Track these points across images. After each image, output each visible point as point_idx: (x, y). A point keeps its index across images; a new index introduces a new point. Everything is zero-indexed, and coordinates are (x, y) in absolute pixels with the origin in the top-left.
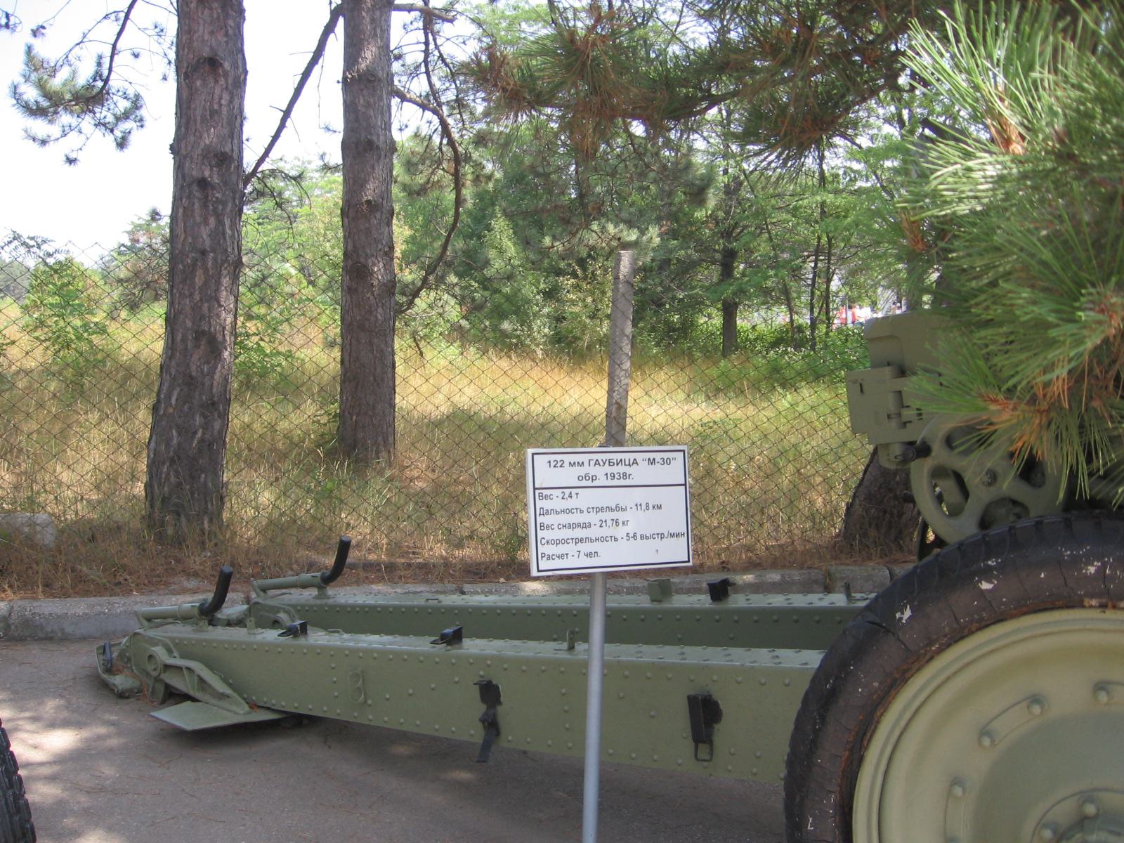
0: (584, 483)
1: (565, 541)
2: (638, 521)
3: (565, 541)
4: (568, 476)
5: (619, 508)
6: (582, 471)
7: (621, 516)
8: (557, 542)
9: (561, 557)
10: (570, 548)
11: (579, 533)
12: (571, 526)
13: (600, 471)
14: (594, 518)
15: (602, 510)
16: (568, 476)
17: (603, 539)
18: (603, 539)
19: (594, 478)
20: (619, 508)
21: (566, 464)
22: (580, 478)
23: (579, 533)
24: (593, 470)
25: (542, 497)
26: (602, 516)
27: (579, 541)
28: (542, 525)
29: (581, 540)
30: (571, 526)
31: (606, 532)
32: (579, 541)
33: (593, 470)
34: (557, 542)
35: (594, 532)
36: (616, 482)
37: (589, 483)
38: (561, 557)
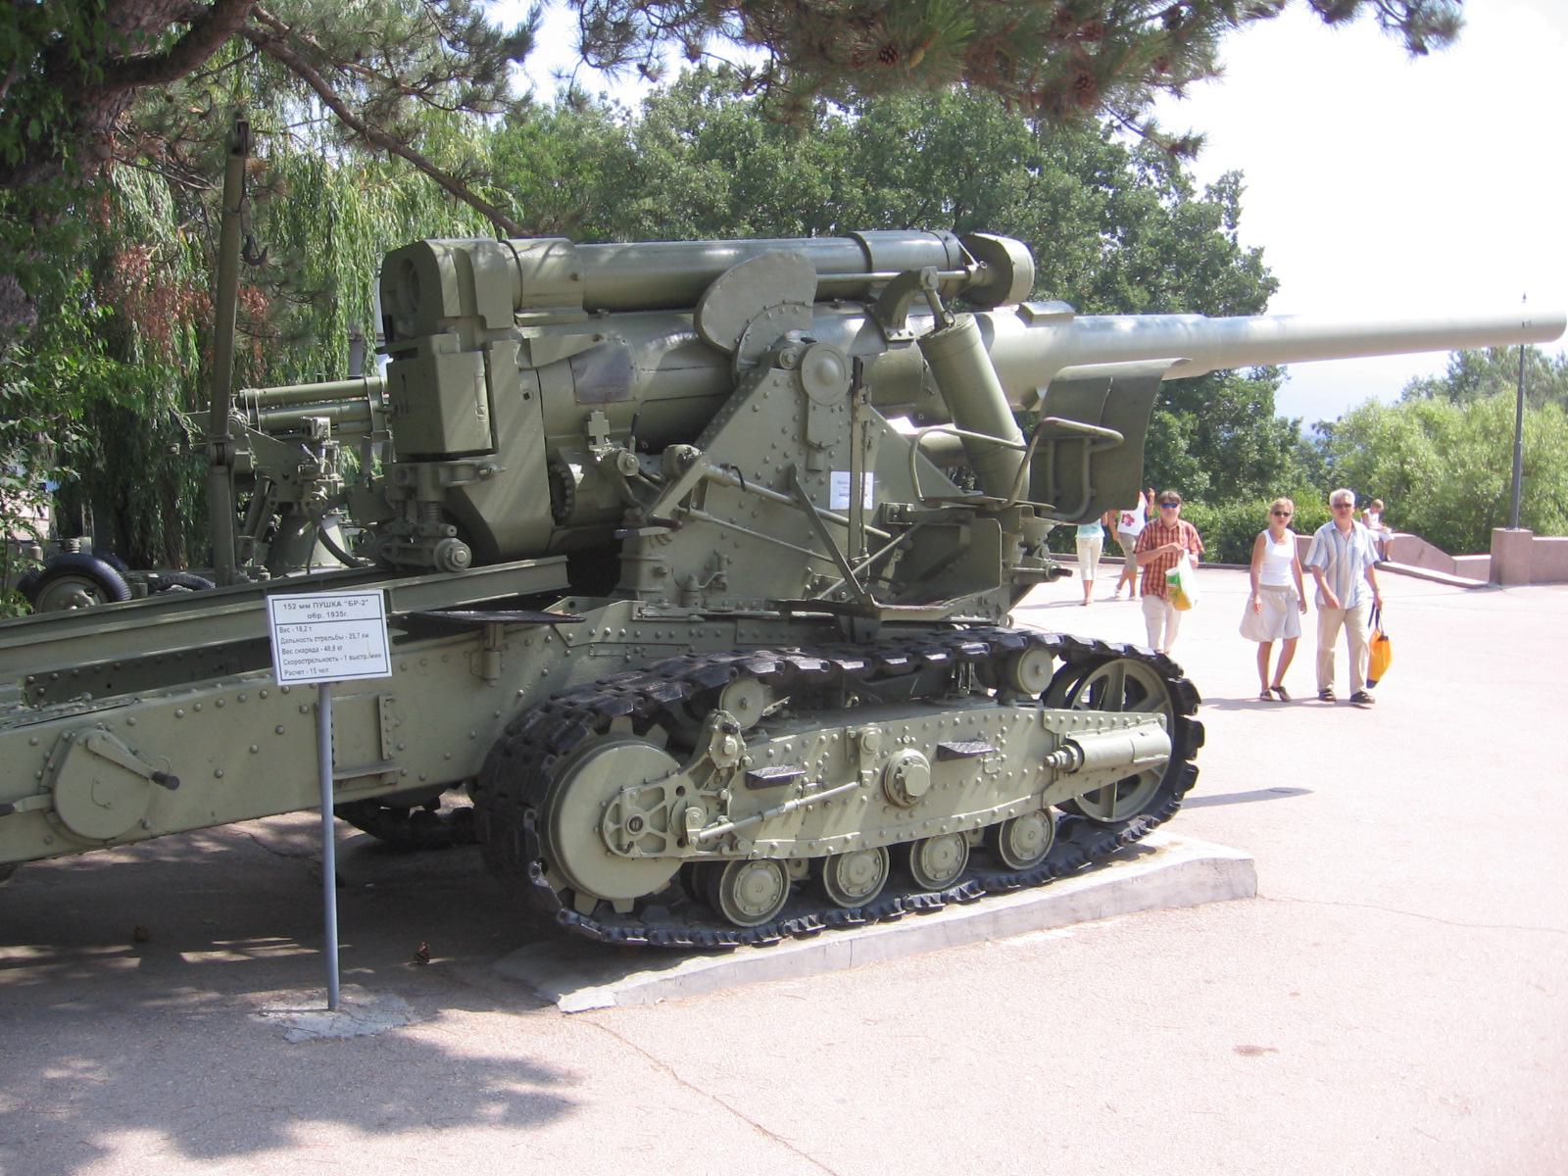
0: (312, 620)
2: (350, 648)
4: (302, 615)
5: (337, 638)
6: (311, 611)
7: (337, 643)
10: (305, 667)
11: (310, 656)
13: (323, 611)
14: (321, 645)
15: (325, 638)
16: (302, 615)
19: (319, 616)
20: (337, 638)
21: (297, 607)
22: (309, 616)
23: (310, 656)
24: (317, 611)
25: (281, 631)
26: (326, 643)
27: (310, 661)
28: (284, 650)
29: (312, 661)
31: (328, 654)
32: (310, 661)
33: (317, 611)
35: (322, 654)
36: (335, 619)
37: (316, 620)
38: (299, 673)
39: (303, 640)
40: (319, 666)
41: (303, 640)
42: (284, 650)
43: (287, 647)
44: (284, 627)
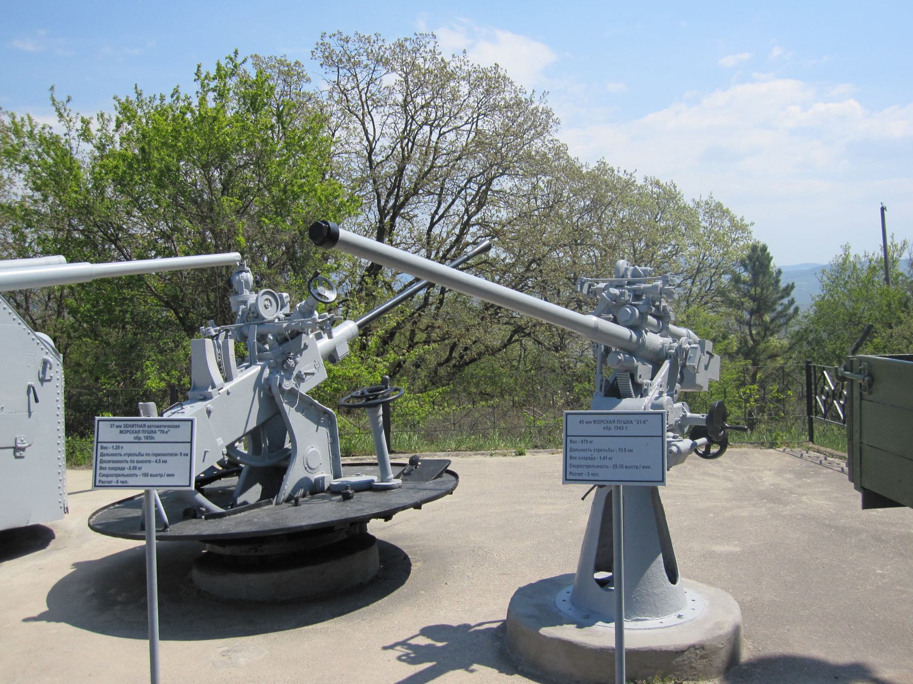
1: (581, 466)
3: (581, 466)
5: (610, 450)
7: (609, 455)
8: (578, 466)
9: (579, 474)
11: (589, 462)
12: (586, 458)
14: (596, 455)
17: (602, 467)
18: (602, 467)
20: (610, 450)
23: (589, 462)
26: (603, 454)
27: (588, 467)
28: (571, 457)
30: (586, 458)
32: (588, 467)
34: (578, 466)
38: (579, 474)
39: (585, 450)
40: (591, 470)
41: (585, 450)
42: (571, 457)
43: (574, 454)
44: (574, 439)
